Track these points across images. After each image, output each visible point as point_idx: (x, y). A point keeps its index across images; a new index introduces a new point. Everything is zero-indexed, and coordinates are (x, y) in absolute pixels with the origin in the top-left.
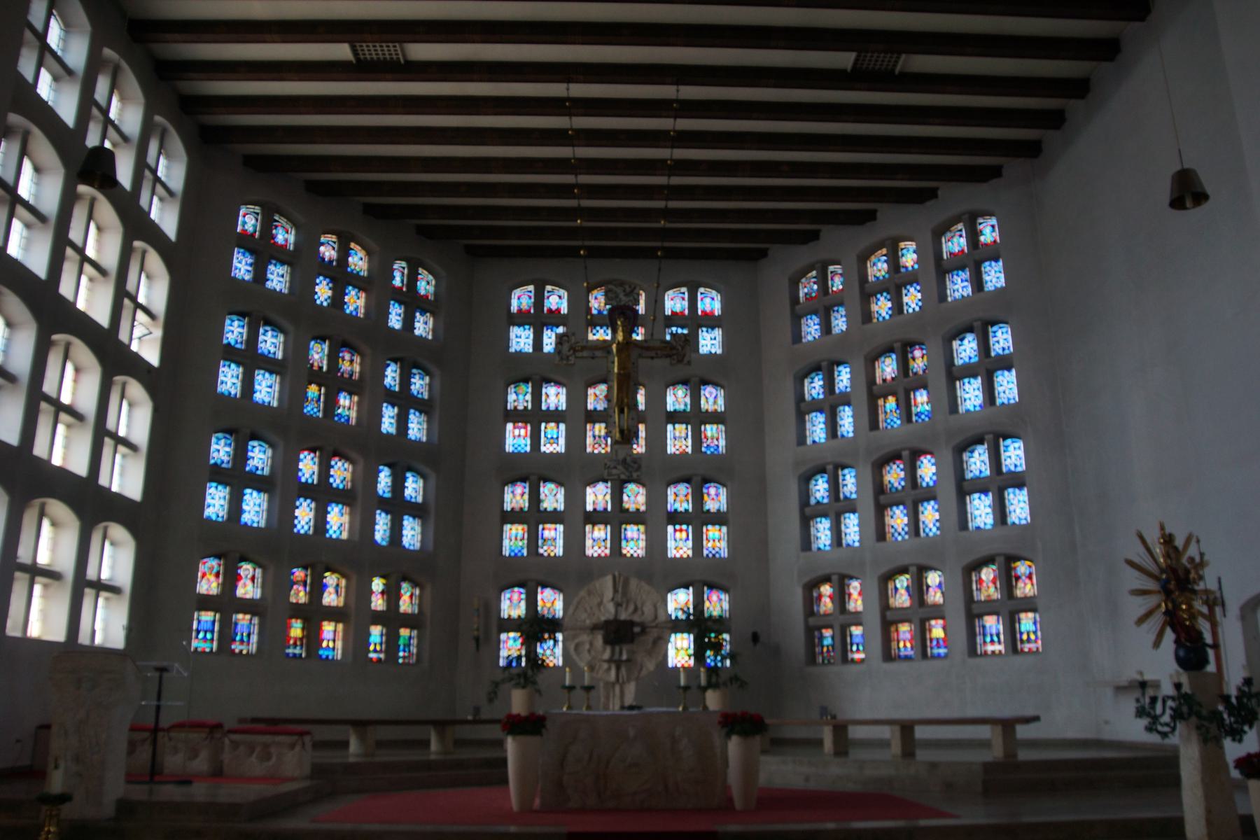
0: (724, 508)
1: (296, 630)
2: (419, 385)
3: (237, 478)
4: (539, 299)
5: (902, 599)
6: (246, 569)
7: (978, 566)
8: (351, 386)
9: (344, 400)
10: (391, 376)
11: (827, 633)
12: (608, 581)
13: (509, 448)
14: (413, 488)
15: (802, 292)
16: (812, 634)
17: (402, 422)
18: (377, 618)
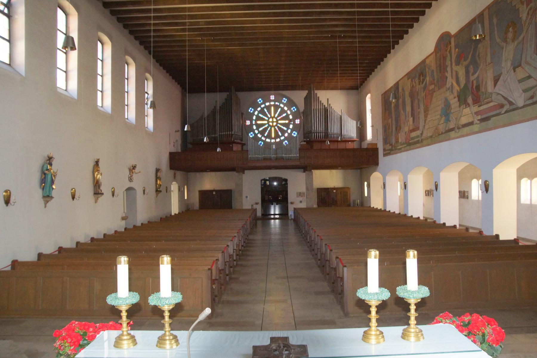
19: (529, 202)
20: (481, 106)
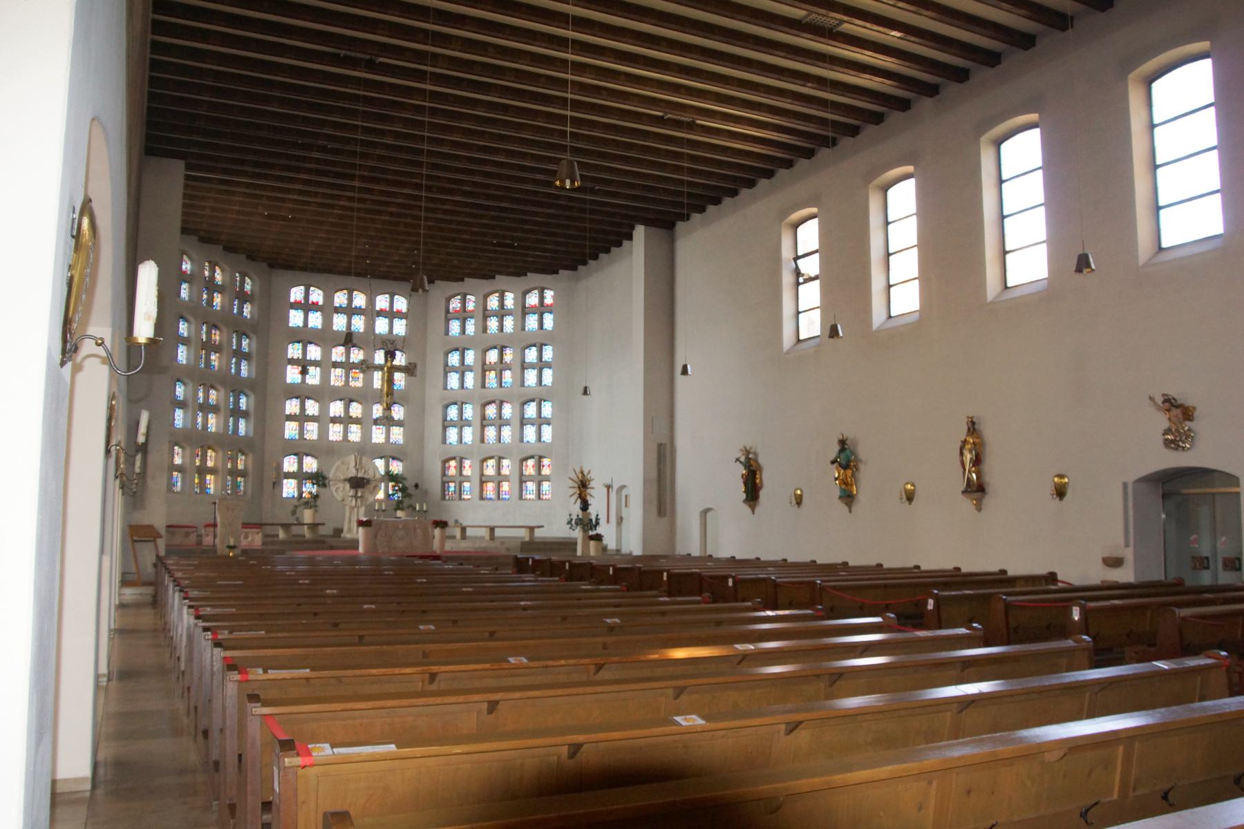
5: (490, 470)
7: (526, 459)
11: (452, 485)
13: (289, 380)
16: (444, 484)
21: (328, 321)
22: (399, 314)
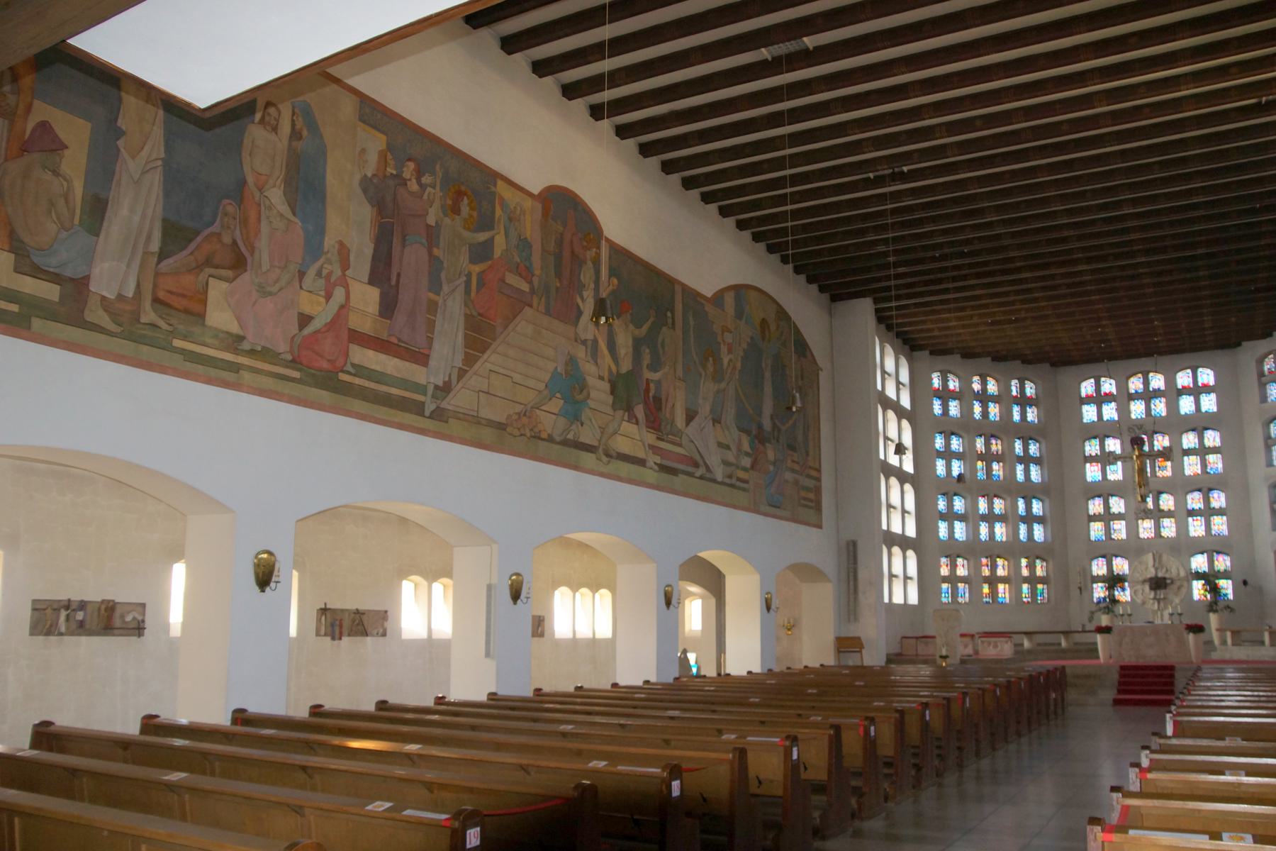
0: (1224, 505)
1: (986, 589)
2: (1034, 449)
3: (950, 516)
4: (1098, 386)
6: (960, 561)
8: (998, 458)
9: (995, 466)
10: (1018, 446)
12: (1150, 556)
13: (1089, 479)
14: (1037, 508)
15: (1266, 368)
17: (1027, 472)
18: (1026, 580)
19: (423, 634)
20: (662, 440)
21: (1124, 411)
22: (1207, 389)
